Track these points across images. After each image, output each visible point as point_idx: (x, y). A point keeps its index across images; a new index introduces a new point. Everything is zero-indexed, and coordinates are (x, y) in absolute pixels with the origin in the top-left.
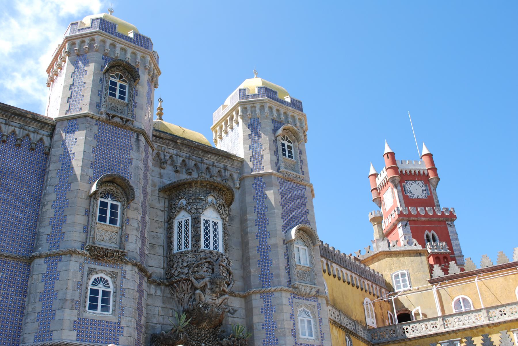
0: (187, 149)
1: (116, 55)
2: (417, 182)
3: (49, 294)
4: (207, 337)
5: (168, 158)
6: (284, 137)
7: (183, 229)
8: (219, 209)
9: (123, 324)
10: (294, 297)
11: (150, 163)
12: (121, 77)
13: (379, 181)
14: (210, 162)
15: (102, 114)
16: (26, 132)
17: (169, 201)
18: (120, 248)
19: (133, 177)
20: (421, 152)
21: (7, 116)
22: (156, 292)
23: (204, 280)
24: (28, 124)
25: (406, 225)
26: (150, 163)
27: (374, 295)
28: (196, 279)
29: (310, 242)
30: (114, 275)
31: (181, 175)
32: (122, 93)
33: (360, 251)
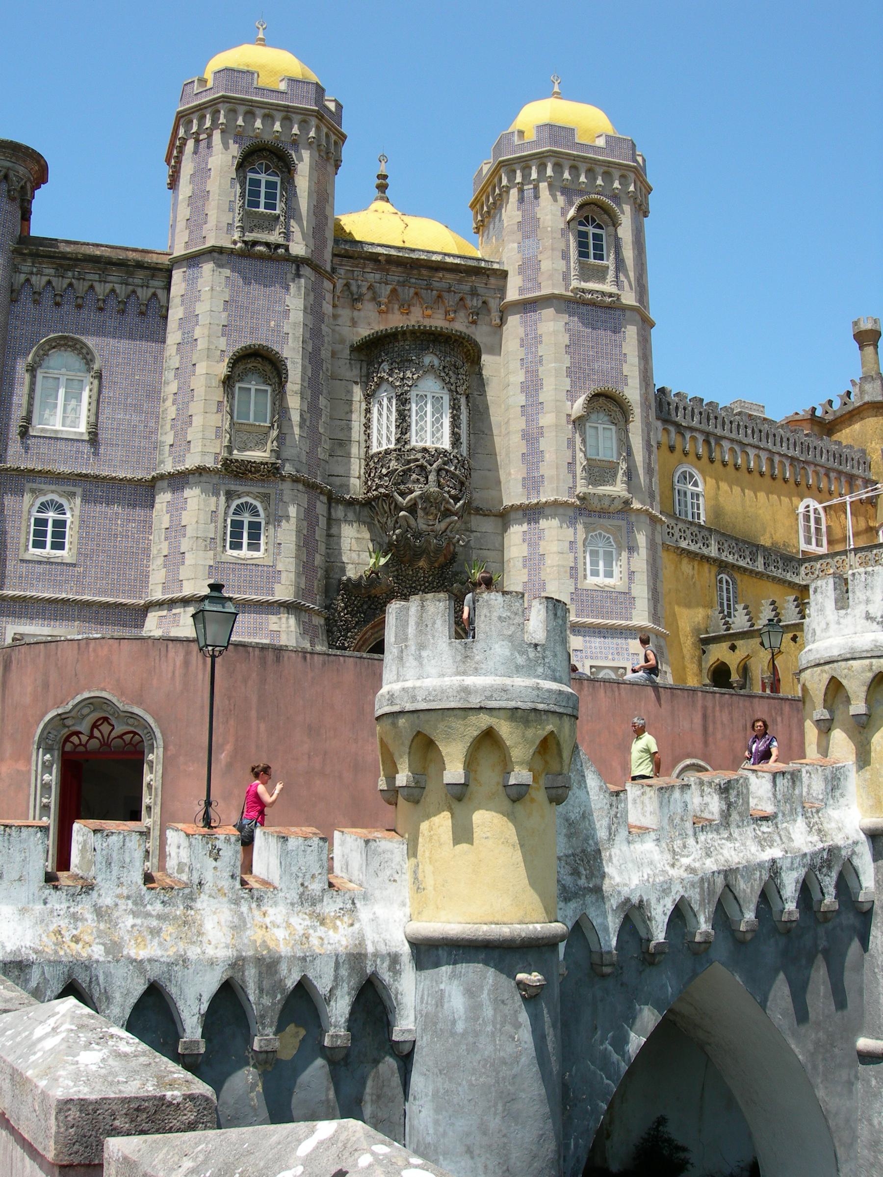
0: (400, 269)
3: (176, 530)
4: (428, 582)
5: (364, 290)
6: (586, 218)
8: (442, 374)
9: (280, 567)
10: (580, 514)
11: (327, 308)
14: (443, 285)
15: (235, 243)
16: (130, 288)
17: (368, 365)
19: (290, 340)
21: (100, 269)
22: (346, 515)
23: (413, 495)
24: (131, 274)
26: (327, 308)
28: (403, 494)
29: (619, 416)
30: (265, 498)
31: (390, 316)
32: (271, 196)
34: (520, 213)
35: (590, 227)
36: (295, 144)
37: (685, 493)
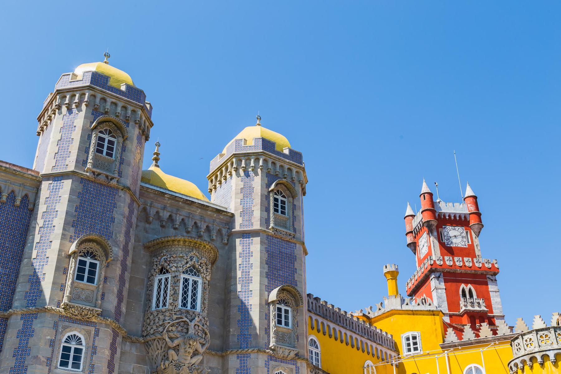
1: (106, 110)
2: (457, 228)
6: (278, 191)
7: (163, 286)
8: (200, 267)
10: (271, 360)
11: (134, 220)
12: (110, 132)
13: (415, 223)
18: (95, 307)
20: (464, 194)
25: (439, 277)
27: (378, 358)
28: (171, 338)
29: (294, 303)
33: (371, 308)
34: (242, 183)
35: (280, 197)
36: (127, 122)
37: (312, 352)
